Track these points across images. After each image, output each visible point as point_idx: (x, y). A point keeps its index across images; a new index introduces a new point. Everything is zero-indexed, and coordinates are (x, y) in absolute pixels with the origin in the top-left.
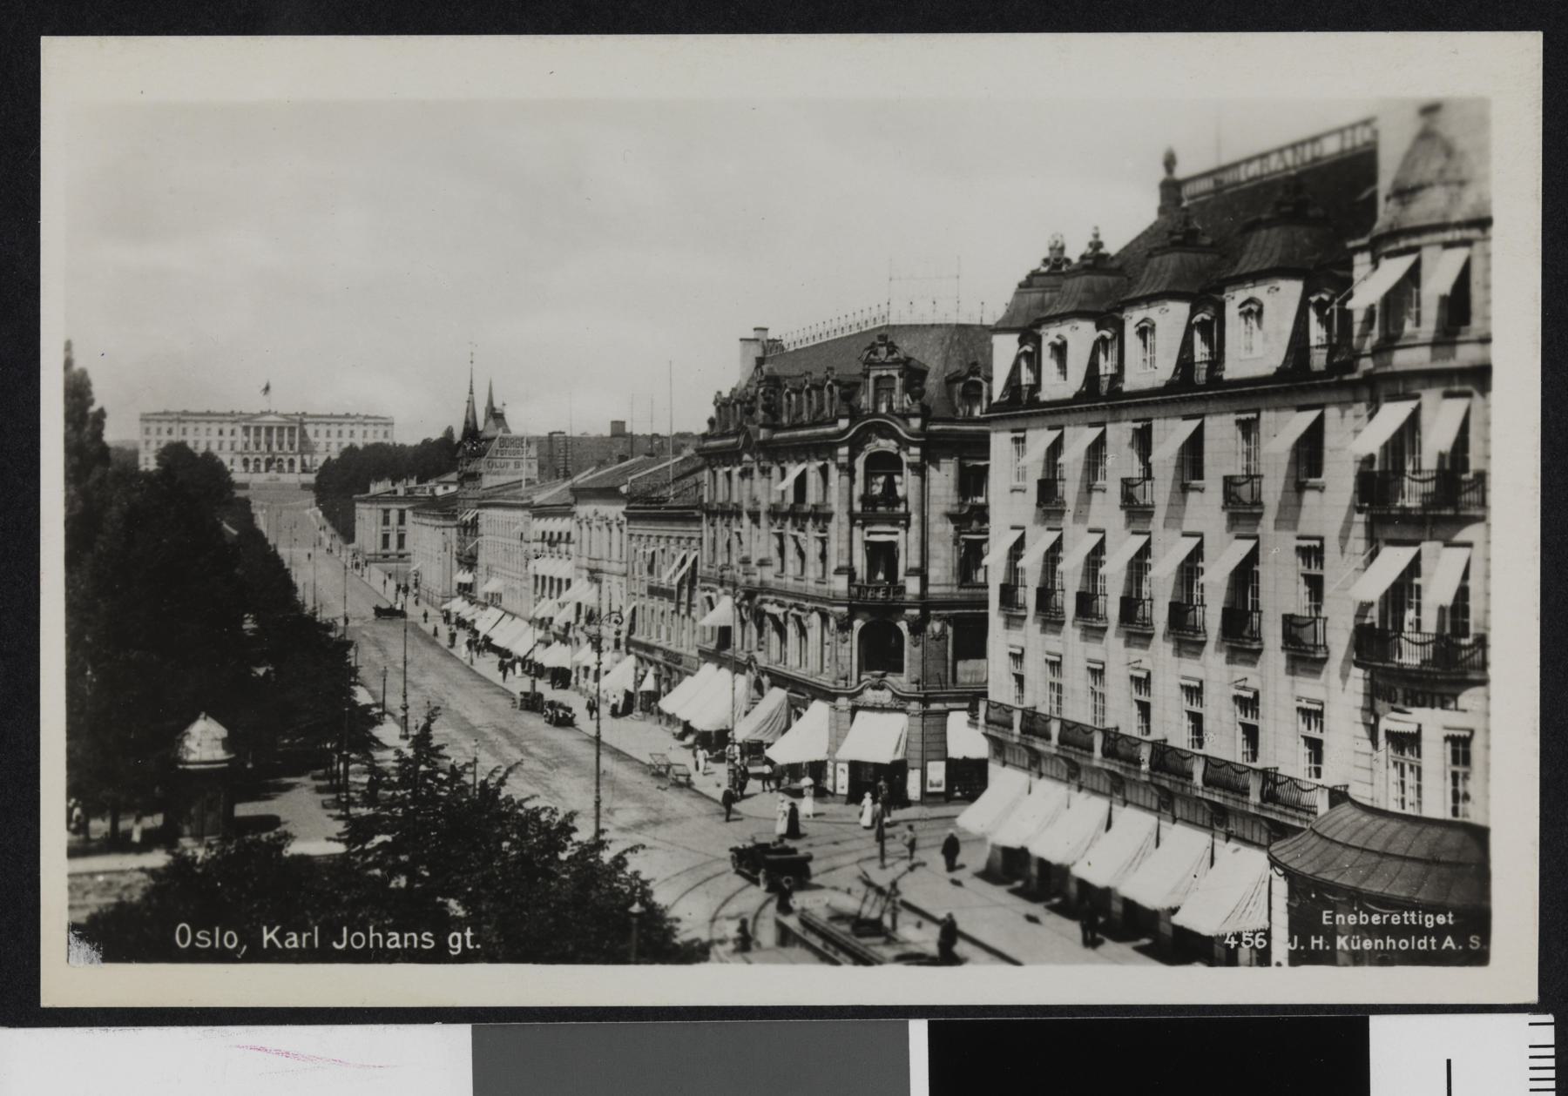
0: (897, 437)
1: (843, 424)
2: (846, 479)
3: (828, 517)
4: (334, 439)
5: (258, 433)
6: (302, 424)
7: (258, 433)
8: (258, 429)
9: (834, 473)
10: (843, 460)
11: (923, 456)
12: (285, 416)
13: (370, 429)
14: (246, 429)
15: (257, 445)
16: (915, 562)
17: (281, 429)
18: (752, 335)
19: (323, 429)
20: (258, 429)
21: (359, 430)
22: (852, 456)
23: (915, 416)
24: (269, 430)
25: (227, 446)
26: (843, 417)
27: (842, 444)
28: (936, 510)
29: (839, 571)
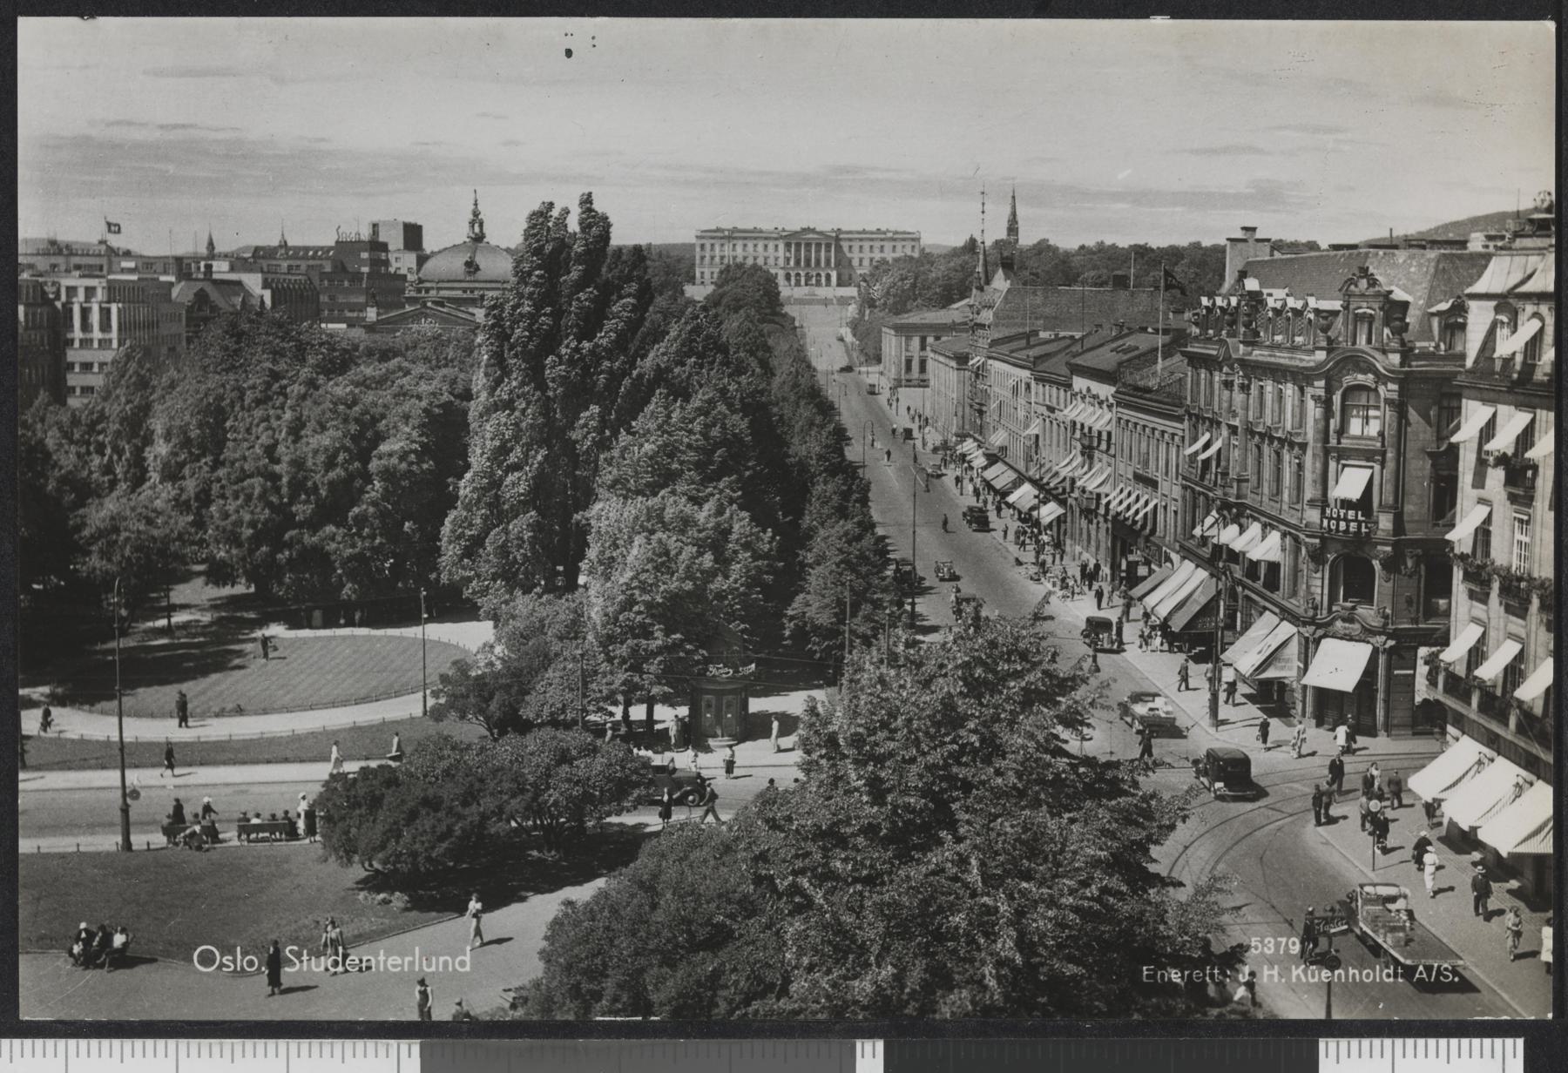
0: (1376, 373)
1: (1321, 356)
2: (1319, 412)
3: (1303, 446)
4: (867, 255)
5: (798, 250)
6: (837, 239)
7: (798, 250)
8: (798, 245)
9: (1310, 404)
10: (1322, 393)
11: (1401, 392)
12: (821, 233)
13: (899, 245)
14: (788, 245)
15: (798, 262)
16: (1389, 498)
17: (818, 245)
18: (1240, 235)
19: (856, 245)
20: (798, 245)
21: (888, 245)
22: (1329, 390)
23: (1394, 351)
24: (808, 245)
25: (771, 261)
26: (1322, 349)
27: (1318, 377)
28: (1412, 447)
29: (1312, 503)
